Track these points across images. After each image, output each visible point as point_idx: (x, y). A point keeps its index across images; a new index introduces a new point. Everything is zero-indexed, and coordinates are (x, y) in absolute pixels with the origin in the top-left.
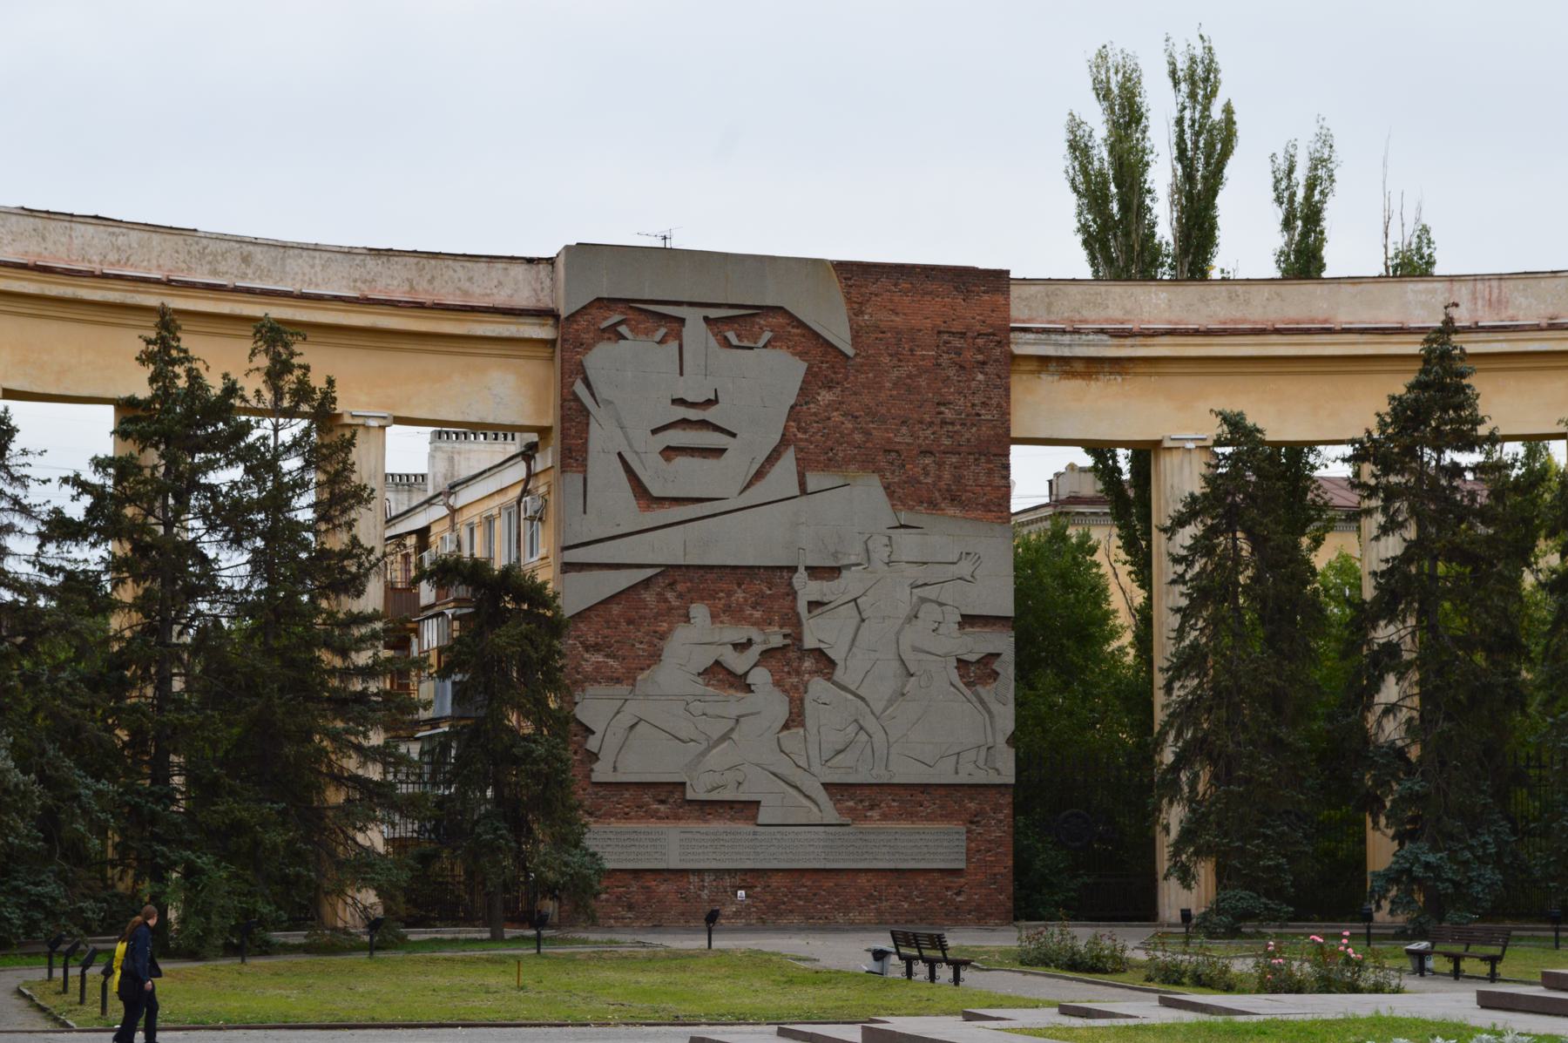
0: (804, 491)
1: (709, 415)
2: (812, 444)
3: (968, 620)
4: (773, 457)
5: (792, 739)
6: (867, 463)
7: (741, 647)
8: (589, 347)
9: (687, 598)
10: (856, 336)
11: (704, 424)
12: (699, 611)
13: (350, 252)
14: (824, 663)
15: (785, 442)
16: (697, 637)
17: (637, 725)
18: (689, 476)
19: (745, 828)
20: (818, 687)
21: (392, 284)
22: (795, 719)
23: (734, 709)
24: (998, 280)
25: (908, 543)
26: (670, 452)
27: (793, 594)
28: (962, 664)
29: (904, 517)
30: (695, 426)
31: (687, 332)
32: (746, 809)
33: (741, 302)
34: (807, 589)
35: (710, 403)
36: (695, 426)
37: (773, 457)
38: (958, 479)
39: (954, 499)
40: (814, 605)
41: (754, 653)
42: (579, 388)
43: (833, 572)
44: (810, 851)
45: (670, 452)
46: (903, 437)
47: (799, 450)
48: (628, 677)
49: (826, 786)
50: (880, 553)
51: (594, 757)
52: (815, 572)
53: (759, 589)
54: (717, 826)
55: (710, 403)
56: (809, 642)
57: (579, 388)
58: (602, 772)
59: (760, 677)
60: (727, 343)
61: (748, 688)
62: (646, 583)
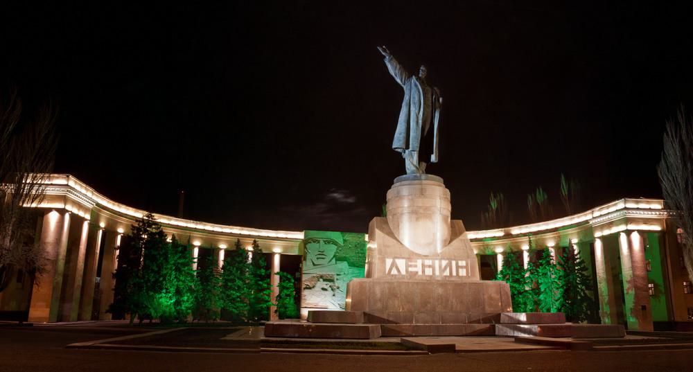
0: (336, 263)
26: (318, 258)
45: (318, 258)
59: (330, 289)
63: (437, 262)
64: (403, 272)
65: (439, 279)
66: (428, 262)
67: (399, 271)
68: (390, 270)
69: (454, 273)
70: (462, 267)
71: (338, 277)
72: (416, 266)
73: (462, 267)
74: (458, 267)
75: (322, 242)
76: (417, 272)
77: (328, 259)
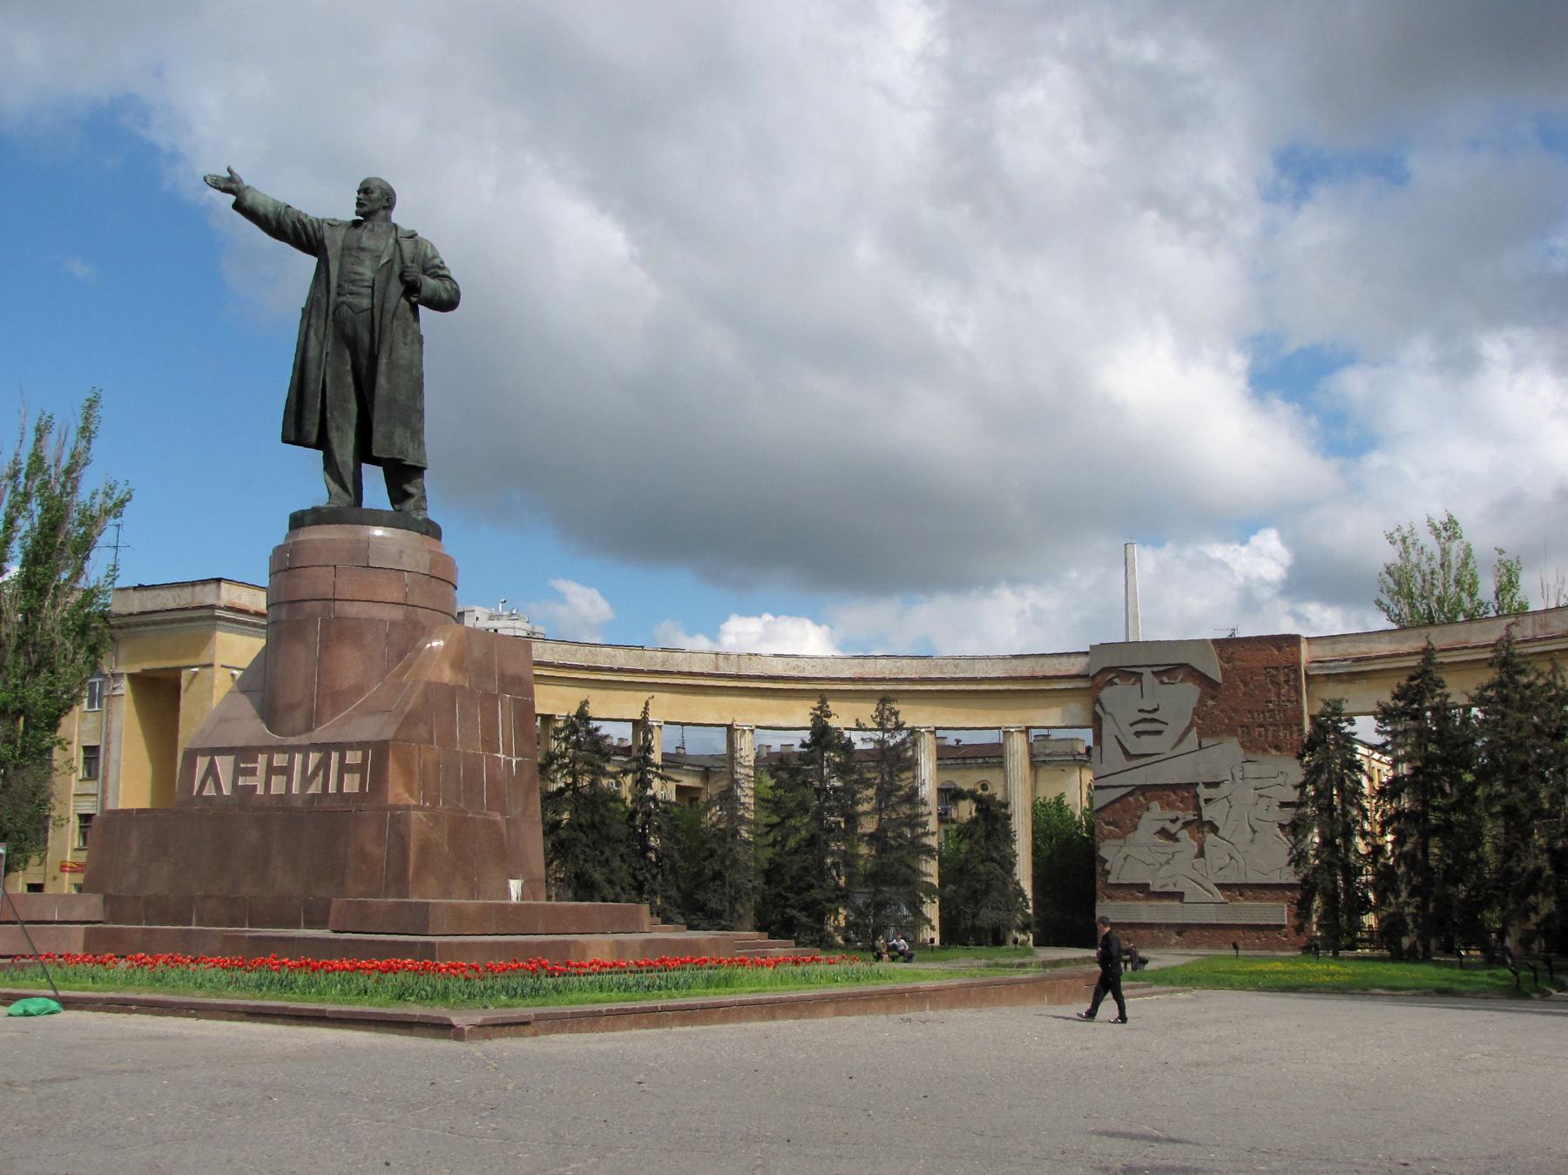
1: (1154, 716)
2: (1207, 725)
3: (1283, 805)
4: (1185, 734)
5: (1199, 862)
6: (1231, 732)
7: (1174, 821)
8: (1101, 689)
9: (1148, 800)
10: (1224, 672)
11: (1153, 720)
12: (1155, 805)
13: (1004, 658)
14: (1214, 829)
15: (1192, 724)
16: (1155, 815)
17: (1127, 859)
18: (1147, 744)
19: (1177, 903)
20: (1210, 837)
21: (1024, 669)
22: (1201, 853)
23: (1170, 850)
24: (1293, 640)
25: (1251, 770)
26: (1138, 734)
27: (1197, 796)
28: (1281, 826)
29: (1251, 757)
30: (1149, 723)
31: (1144, 679)
32: (1179, 896)
33: (1172, 664)
34: (1204, 793)
35: (1155, 710)
36: (1149, 723)
37: (1185, 734)
38: (1275, 737)
39: (1277, 748)
40: (1207, 801)
41: (1179, 824)
42: (1098, 708)
43: (1216, 785)
44: (1209, 916)
45: (1138, 734)
46: (1247, 719)
47: (1199, 728)
48: (1123, 836)
49: (1217, 885)
50: (1238, 775)
51: (1108, 873)
52: (1208, 785)
53: (1184, 792)
54: (1166, 903)
55: (1155, 710)
56: (1205, 818)
57: (1098, 708)
58: (1112, 879)
60: (1162, 683)
61: (1177, 840)
62: (1131, 793)
63: (298, 757)
64: (226, 791)
65: (299, 803)
66: (279, 760)
67: (218, 787)
68: (203, 783)
69: (332, 789)
70: (351, 769)
71: (1212, 792)
72: (253, 772)
73: (351, 769)
74: (344, 768)
75: (1147, 672)
76: (255, 787)
77: (1170, 736)
